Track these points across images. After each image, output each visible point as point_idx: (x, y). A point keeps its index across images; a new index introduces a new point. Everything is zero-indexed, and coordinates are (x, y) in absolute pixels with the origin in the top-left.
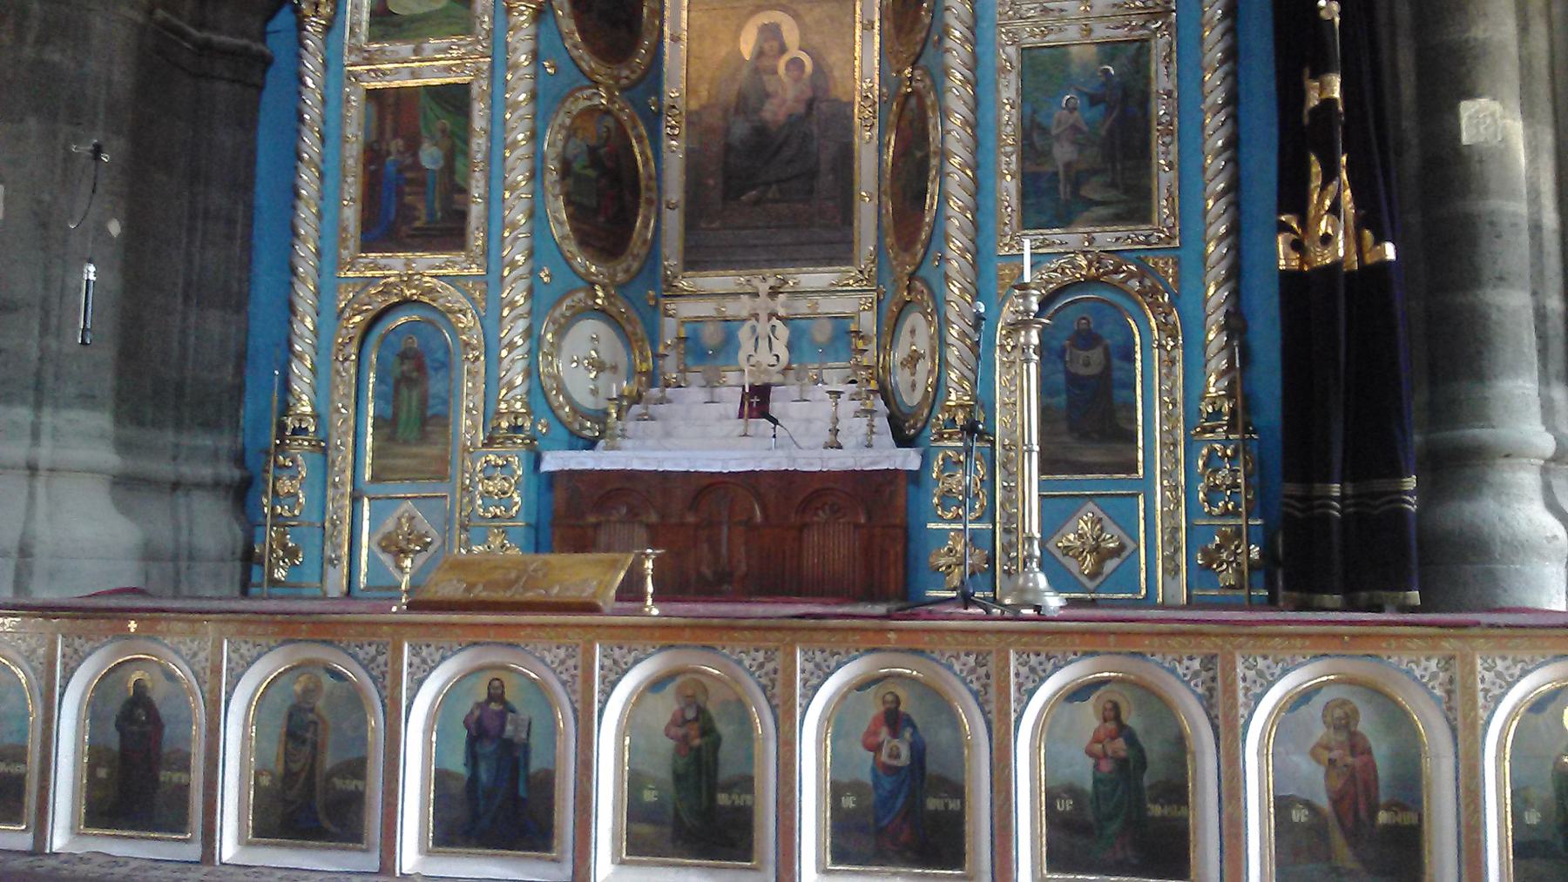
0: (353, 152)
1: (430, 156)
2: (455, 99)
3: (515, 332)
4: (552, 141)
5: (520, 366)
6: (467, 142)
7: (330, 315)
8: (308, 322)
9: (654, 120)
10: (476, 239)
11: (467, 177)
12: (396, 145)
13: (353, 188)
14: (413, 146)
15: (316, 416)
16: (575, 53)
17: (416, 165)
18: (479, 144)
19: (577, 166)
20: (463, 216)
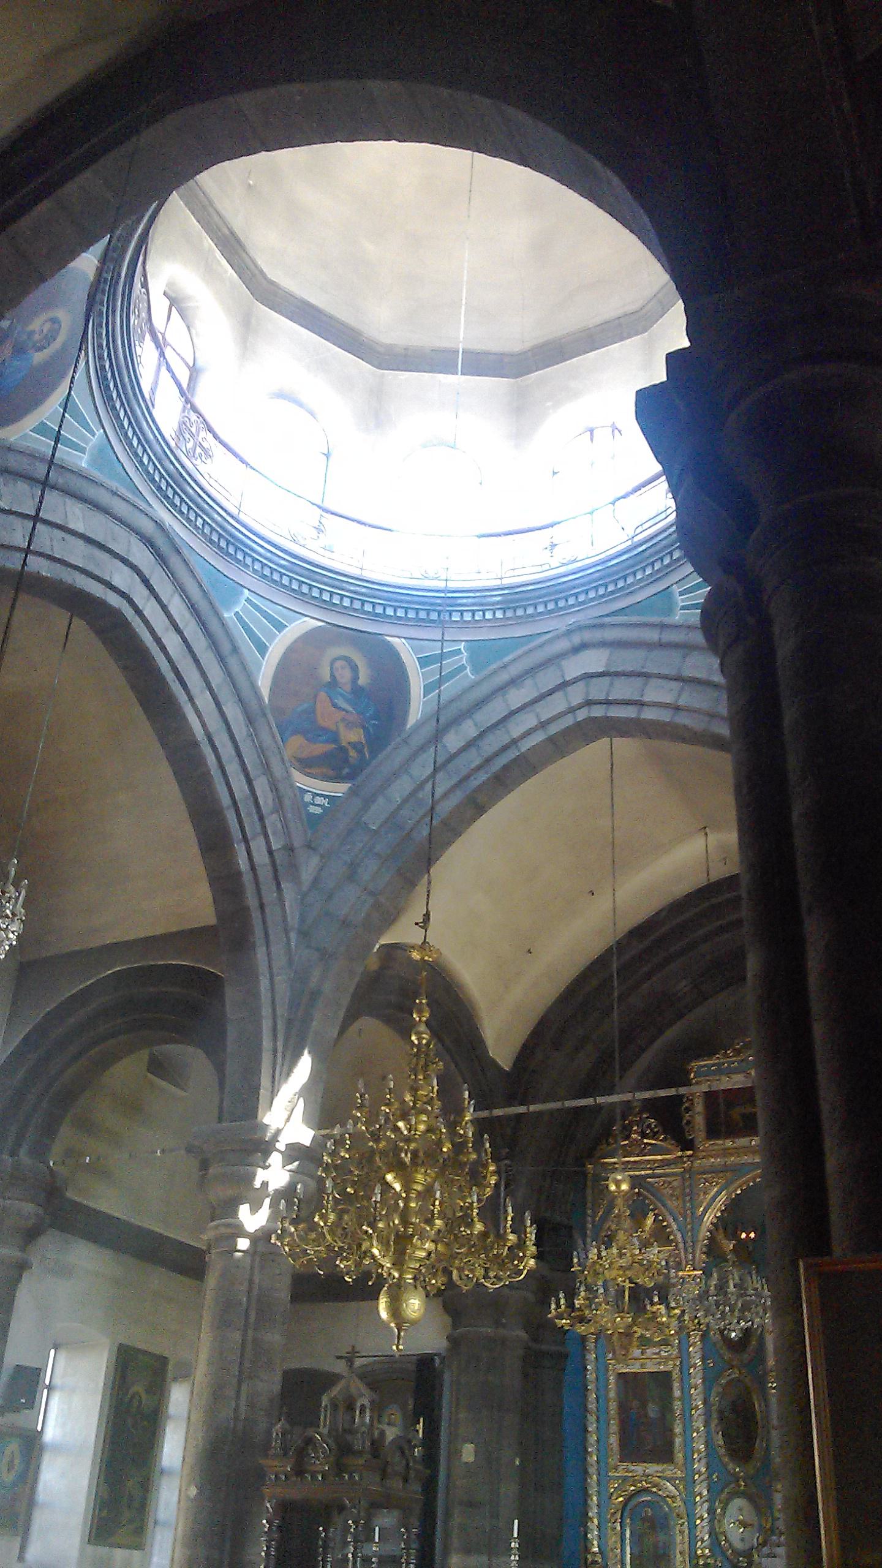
0: (613, 1406)
1: (653, 1411)
2: (663, 1380)
3: (702, 1511)
4: (714, 1399)
5: (707, 1529)
6: (671, 1404)
7: (605, 1498)
8: (595, 1498)
9: (762, 1382)
10: (679, 1456)
11: (672, 1424)
12: (635, 1404)
13: (614, 1426)
14: (644, 1405)
15: (601, 1552)
16: (722, 1352)
17: (646, 1415)
18: (677, 1405)
19: (726, 1414)
20: (671, 1444)
